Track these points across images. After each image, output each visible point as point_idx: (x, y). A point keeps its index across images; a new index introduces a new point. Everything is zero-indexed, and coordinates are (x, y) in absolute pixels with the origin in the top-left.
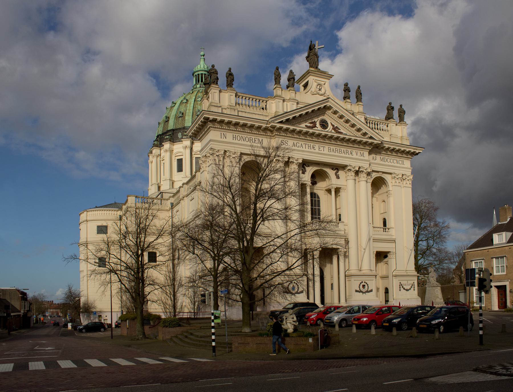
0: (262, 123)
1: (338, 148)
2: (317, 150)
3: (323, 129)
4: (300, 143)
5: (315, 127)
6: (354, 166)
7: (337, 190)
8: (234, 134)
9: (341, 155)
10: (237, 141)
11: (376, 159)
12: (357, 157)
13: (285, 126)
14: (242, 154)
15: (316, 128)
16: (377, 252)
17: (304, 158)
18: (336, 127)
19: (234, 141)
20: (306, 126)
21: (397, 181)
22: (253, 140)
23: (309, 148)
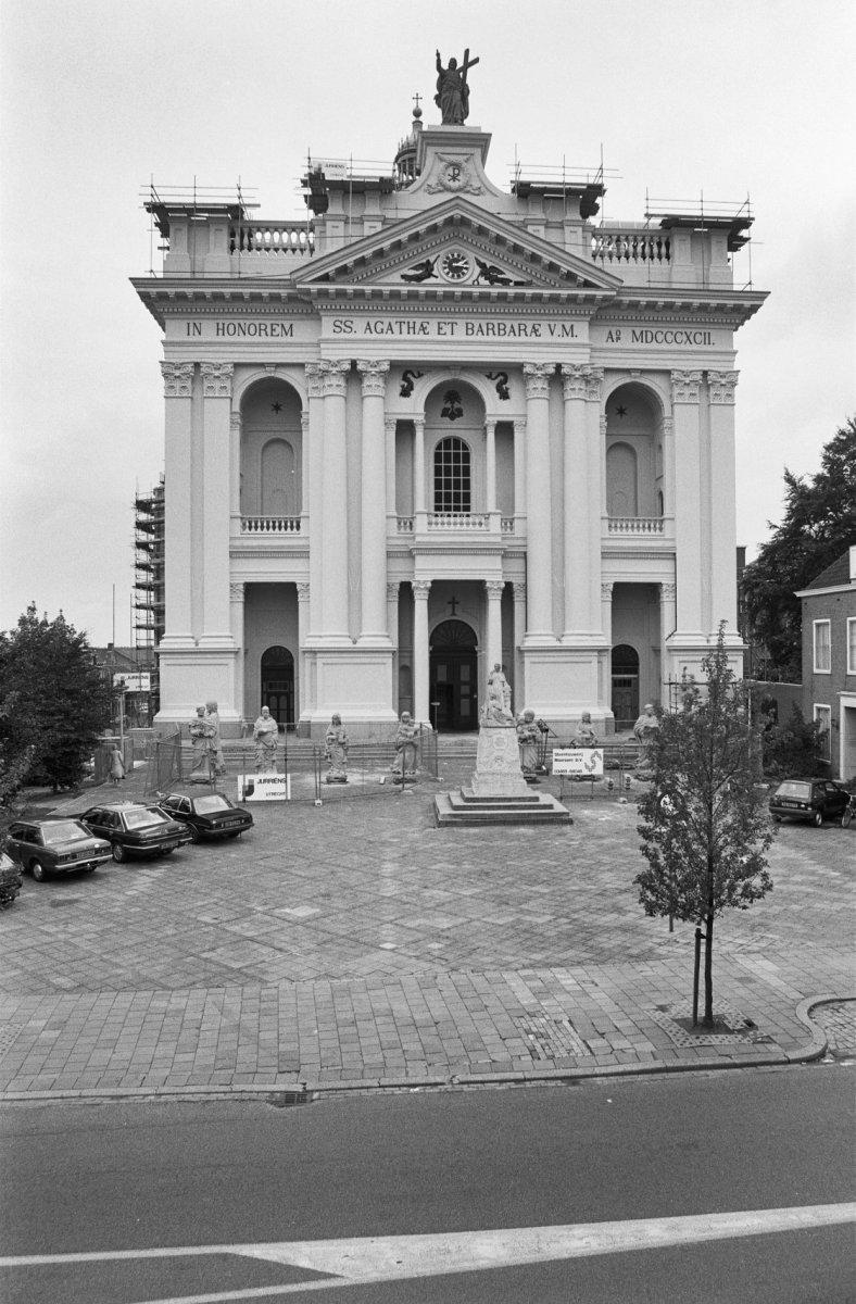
0: (279, 287)
2: (433, 335)
4: (386, 321)
5: (429, 274)
6: (540, 362)
7: (505, 430)
8: (221, 322)
9: (505, 339)
10: (227, 338)
11: (618, 339)
12: (555, 339)
13: (332, 287)
14: (237, 366)
15: (432, 280)
16: (617, 585)
17: (393, 358)
19: (220, 339)
20: (403, 277)
21: (687, 391)
22: (269, 330)
23: (411, 330)
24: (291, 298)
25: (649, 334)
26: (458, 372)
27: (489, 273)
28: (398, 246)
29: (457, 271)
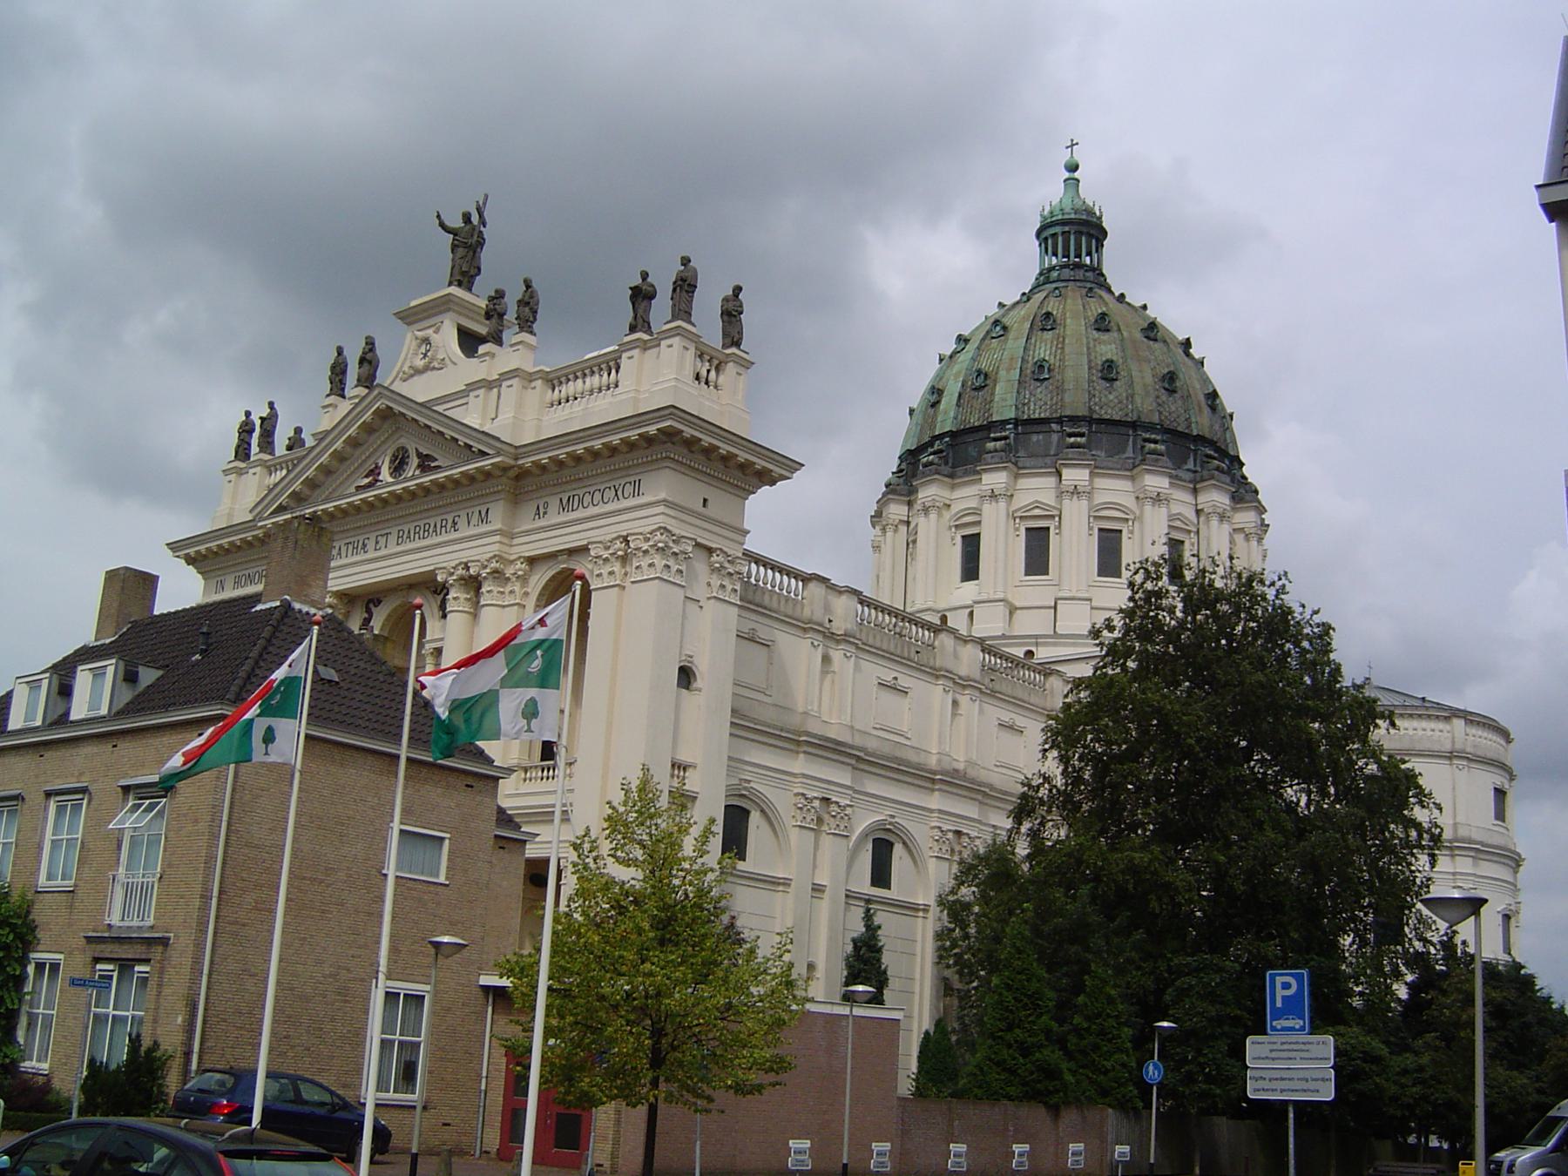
1: (421, 523)
3: (395, 478)
5: (377, 481)
15: (379, 483)
18: (427, 455)
20: (359, 488)
25: (576, 497)
26: (405, 593)
27: (426, 464)
28: (339, 457)
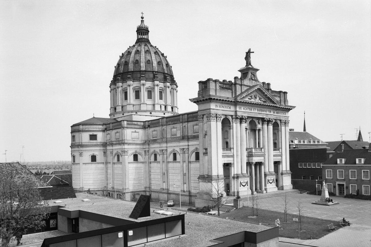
5: (252, 98)
24: (234, 102)
29: (256, 98)
